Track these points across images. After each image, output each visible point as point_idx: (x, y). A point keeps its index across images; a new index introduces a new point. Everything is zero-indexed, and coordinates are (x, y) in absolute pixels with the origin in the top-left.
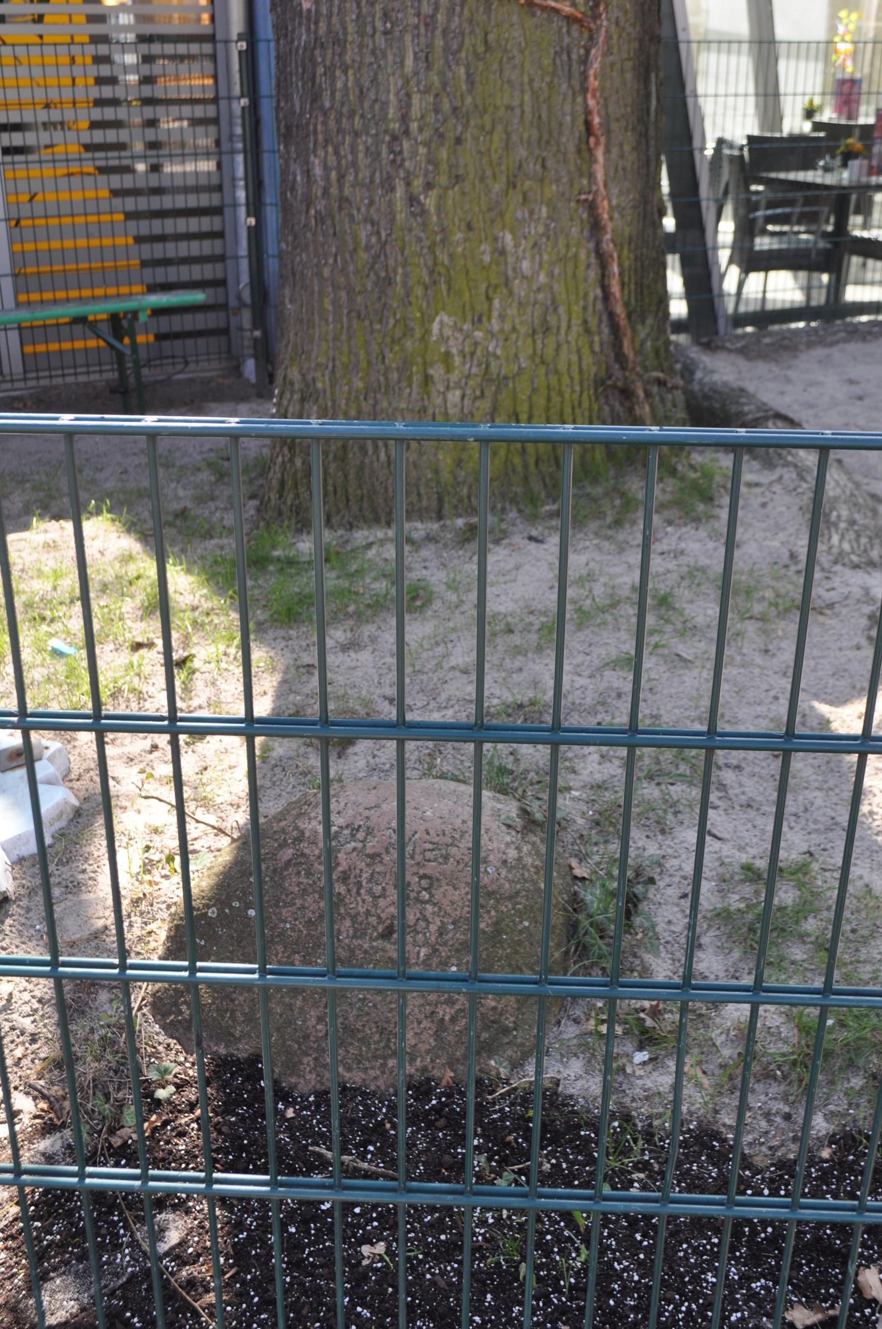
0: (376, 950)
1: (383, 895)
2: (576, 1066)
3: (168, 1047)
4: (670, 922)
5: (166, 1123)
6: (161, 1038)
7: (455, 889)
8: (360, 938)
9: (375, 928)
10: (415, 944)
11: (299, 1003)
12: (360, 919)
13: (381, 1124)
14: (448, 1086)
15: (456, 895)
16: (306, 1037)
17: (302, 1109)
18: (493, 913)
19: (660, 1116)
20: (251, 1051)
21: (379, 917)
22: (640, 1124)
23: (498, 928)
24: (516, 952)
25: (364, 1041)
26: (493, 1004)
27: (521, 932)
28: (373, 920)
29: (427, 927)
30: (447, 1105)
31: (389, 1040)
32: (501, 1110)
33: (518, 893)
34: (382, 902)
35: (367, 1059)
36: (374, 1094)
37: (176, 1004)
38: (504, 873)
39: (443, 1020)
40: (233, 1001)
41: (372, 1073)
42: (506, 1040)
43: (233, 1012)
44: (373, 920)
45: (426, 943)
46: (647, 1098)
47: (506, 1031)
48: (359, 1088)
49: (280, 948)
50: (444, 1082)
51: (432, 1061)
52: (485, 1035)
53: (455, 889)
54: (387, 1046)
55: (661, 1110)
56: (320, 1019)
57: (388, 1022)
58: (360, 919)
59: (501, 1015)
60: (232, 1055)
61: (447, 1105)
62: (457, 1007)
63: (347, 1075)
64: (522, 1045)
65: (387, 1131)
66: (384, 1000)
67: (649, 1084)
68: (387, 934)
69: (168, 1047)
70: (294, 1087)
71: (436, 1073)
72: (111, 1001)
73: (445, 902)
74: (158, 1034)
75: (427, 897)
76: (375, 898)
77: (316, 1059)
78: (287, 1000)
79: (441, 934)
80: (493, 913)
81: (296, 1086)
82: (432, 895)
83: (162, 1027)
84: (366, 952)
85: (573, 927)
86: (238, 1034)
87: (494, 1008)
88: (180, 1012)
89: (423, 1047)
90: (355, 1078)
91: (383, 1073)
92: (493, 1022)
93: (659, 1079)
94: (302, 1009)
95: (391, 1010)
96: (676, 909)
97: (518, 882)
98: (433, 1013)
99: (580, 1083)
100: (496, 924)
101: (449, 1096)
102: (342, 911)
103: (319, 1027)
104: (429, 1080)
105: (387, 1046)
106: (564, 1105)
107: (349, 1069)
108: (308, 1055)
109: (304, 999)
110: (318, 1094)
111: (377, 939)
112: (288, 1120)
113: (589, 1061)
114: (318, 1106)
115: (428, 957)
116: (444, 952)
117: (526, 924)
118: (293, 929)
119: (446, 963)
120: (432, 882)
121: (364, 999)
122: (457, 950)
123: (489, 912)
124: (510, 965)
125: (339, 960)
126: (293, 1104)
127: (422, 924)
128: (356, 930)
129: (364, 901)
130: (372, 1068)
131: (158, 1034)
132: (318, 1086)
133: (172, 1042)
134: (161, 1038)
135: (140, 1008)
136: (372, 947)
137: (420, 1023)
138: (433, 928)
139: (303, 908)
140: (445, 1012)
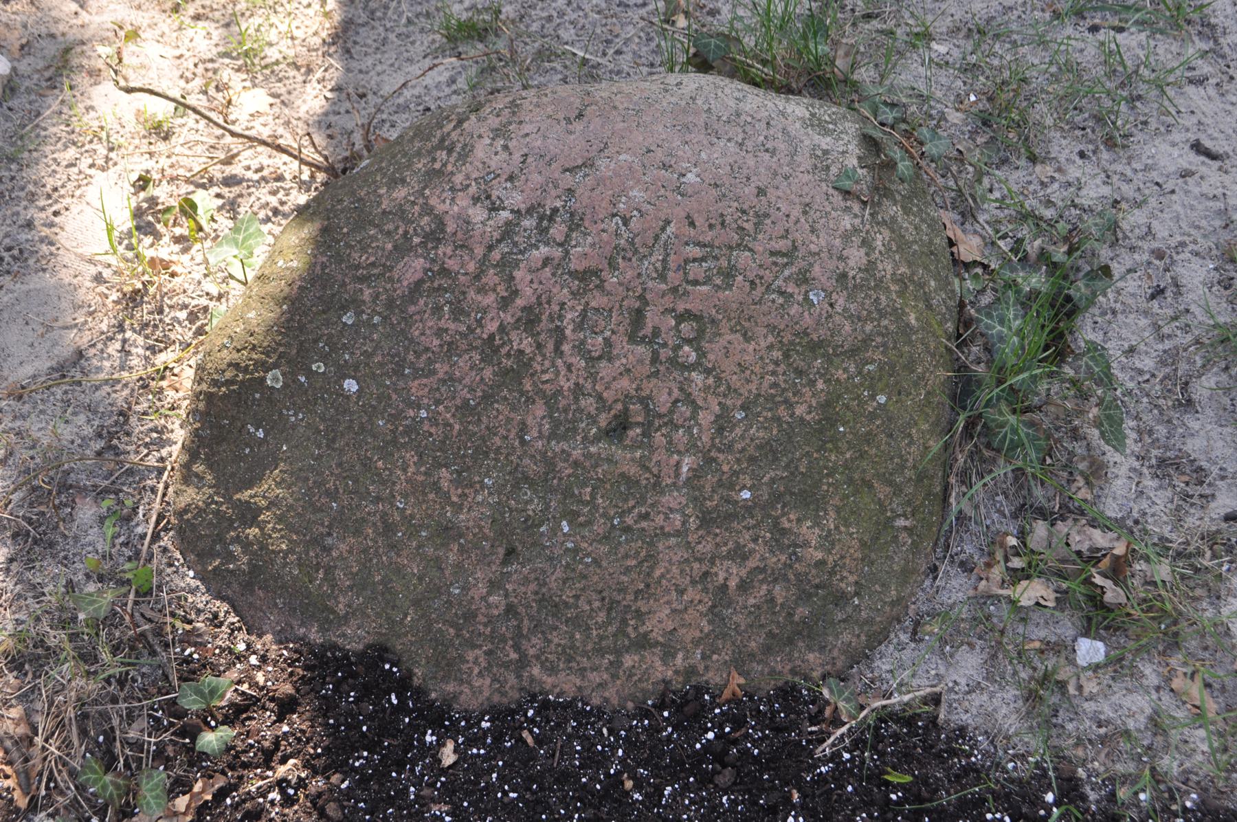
0: (597, 460)
1: (607, 354)
2: (968, 665)
3: (215, 621)
4: (1131, 350)
5: (221, 795)
6: (201, 600)
7: (748, 339)
8: (564, 437)
9: (593, 420)
10: (671, 447)
11: (452, 557)
12: (563, 403)
13: (616, 780)
14: (734, 700)
15: (749, 352)
16: (470, 616)
17: (470, 743)
18: (820, 385)
19: (1126, 779)
20: (370, 640)
21: (600, 398)
22: (1093, 796)
23: (829, 411)
24: (862, 455)
25: (575, 622)
26: (819, 555)
27: (872, 416)
28: (588, 403)
29: (694, 416)
30: (735, 742)
31: (624, 622)
32: (835, 757)
33: (867, 340)
34: (605, 369)
35: (585, 654)
36: (599, 712)
37: (220, 539)
38: (841, 302)
39: (725, 587)
40: (327, 550)
41: (595, 678)
42: (840, 616)
43: (329, 570)
44: (588, 403)
45: (692, 447)
46: (1103, 740)
47: (840, 599)
48: (570, 705)
49: (411, 456)
50: (727, 694)
51: (704, 657)
52: (802, 611)
53: (748, 339)
54: (622, 632)
55: (1131, 768)
56: (494, 586)
57: (622, 590)
58: (563, 403)
59: (832, 573)
60: (334, 647)
61: (735, 742)
62: (752, 563)
63: (549, 681)
64: (869, 621)
65: (627, 794)
66: (614, 550)
67: (1108, 713)
68: (619, 427)
69: (215, 621)
70: (449, 701)
71: (713, 678)
72: (102, 520)
73: (729, 366)
74: (193, 591)
75: (693, 357)
76: (592, 360)
77: (489, 653)
78: (430, 551)
79: (721, 430)
80: (820, 385)
81: (455, 697)
82: (702, 354)
83: (201, 576)
84: (576, 464)
85: (963, 389)
86: (341, 609)
87: (822, 563)
88: (230, 557)
89: (689, 635)
90: (562, 685)
91: (615, 677)
92: (817, 587)
93: (1127, 702)
94: (459, 566)
95: (628, 570)
96: (1143, 322)
97: (869, 318)
98: (706, 574)
99: (978, 699)
100: (827, 405)
101: (739, 723)
102: (528, 386)
103: (493, 599)
104: (699, 690)
105: (622, 632)
106: (954, 753)
107: (552, 670)
108: (474, 647)
109: (462, 550)
110: (497, 714)
111: (597, 439)
112: (444, 771)
113: (994, 657)
114: (498, 739)
115: (696, 474)
116: (727, 463)
117: (882, 399)
118: (433, 420)
119: (731, 484)
120: (702, 326)
121: (576, 550)
122: (752, 460)
123: (812, 383)
124: (850, 481)
125: (526, 478)
126: (453, 731)
127: (684, 409)
128: (556, 424)
129: (569, 367)
130: (594, 669)
131: (193, 591)
132: (496, 698)
133: (222, 607)
134: (201, 600)
135: (156, 537)
136: (588, 456)
137: (681, 592)
138: (705, 418)
139: (450, 379)
140: (730, 573)
